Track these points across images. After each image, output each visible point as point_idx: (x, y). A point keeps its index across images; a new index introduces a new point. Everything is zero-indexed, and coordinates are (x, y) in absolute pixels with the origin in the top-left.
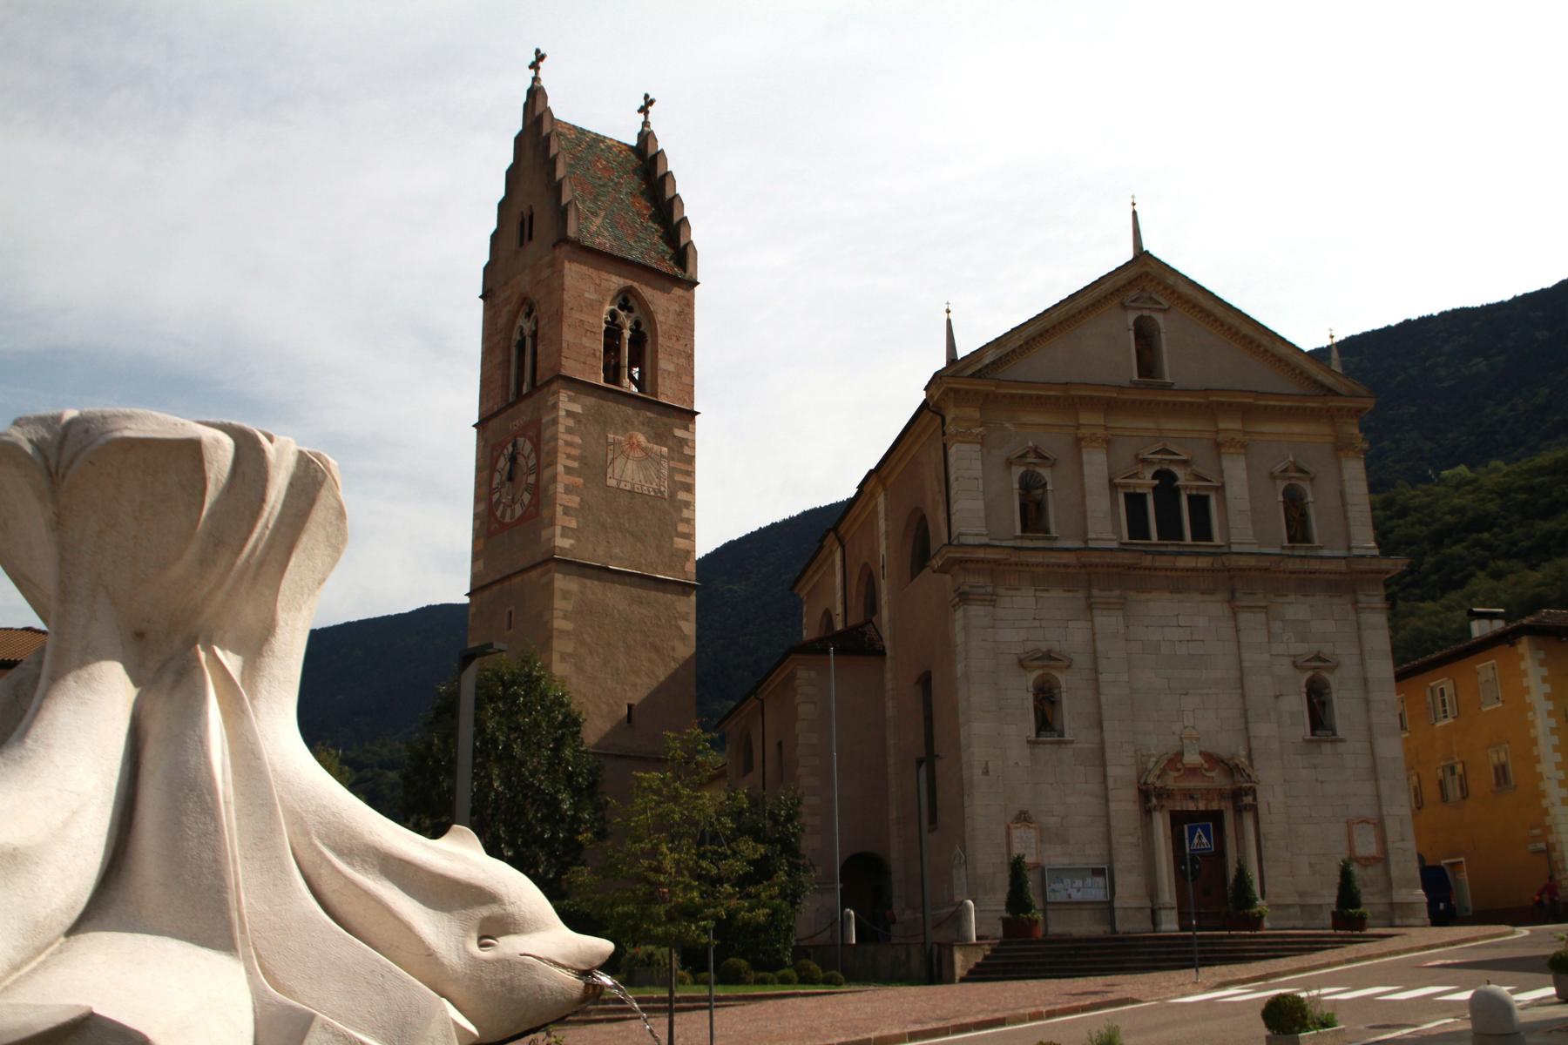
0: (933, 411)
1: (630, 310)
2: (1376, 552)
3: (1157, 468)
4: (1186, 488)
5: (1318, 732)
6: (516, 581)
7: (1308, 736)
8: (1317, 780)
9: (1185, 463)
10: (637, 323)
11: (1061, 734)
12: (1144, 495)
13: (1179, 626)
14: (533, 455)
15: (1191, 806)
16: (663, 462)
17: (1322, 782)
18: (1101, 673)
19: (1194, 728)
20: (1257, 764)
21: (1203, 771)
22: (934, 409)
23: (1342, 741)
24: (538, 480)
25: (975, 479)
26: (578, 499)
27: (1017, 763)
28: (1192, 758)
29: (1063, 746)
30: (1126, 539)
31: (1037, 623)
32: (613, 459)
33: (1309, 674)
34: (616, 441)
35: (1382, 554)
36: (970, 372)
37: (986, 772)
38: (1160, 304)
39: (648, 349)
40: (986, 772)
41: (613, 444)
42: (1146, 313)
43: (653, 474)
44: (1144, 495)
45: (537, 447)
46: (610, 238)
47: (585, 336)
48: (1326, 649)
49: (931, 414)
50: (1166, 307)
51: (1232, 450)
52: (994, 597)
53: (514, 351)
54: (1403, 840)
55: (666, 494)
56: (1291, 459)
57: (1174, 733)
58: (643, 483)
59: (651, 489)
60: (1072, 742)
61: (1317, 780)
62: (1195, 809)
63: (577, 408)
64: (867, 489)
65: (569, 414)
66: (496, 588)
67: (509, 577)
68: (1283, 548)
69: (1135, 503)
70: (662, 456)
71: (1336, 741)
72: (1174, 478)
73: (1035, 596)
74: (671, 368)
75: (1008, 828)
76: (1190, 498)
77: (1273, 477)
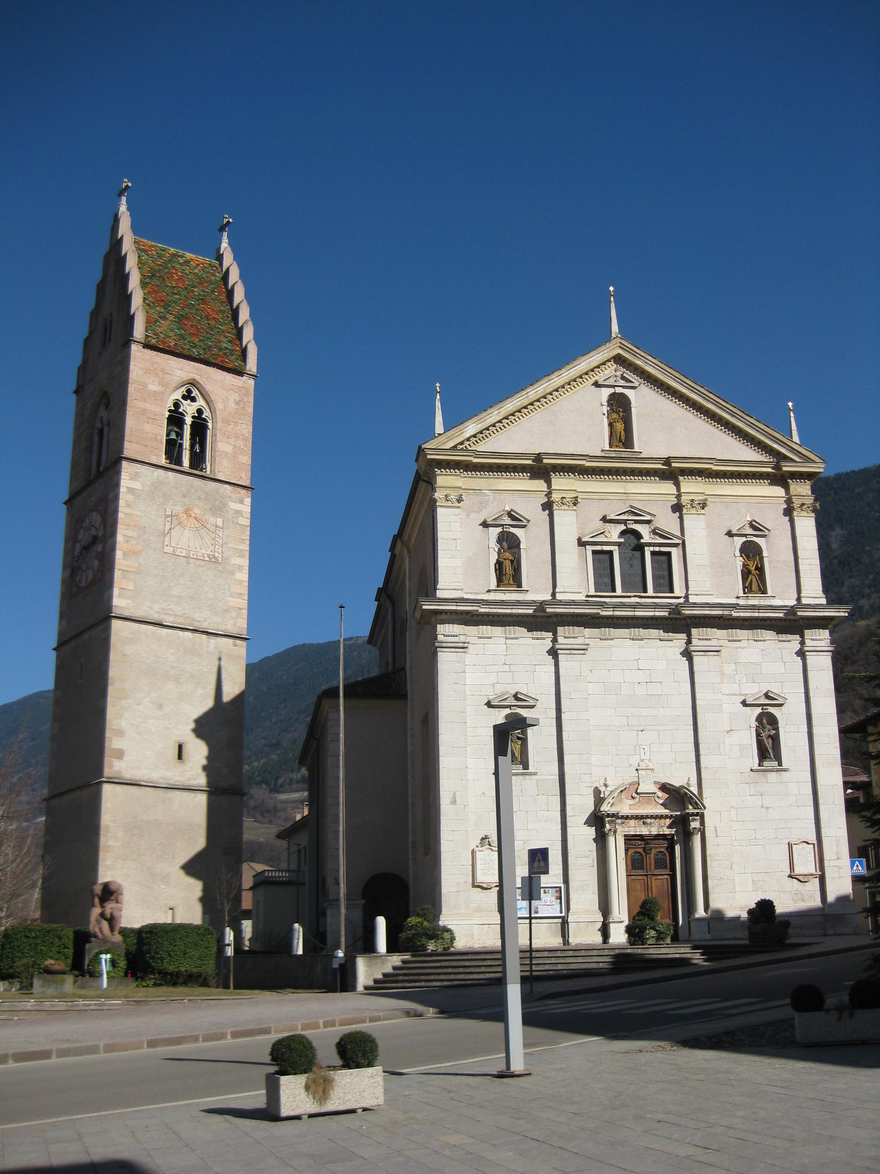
0: (424, 481)
1: (193, 400)
2: (823, 601)
3: (623, 527)
4: (649, 545)
5: (766, 763)
6: (86, 636)
7: (756, 767)
8: (762, 807)
9: (648, 522)
10: (200, 411)
11: (526, 767)
12: (610, 553)
13: (639, 669)
14: (102, 527)
15: (644, 831)
16: (217, 531)
17: (767, 808)
18: (564, 713)
19: (650, 760)
20: (705, 795)
21: (657, 799)
22: (426, 479)
23: (785, 770)
24: (104, 547)
25: (453, 539)
26: (136, 564)
27: (483, 793)
28: (647, 786)
29: (528, 777)
30: (592, 592)
31: (506, 668)
32: (170, 529)
33: (759, 710)
34: (174, 514)
35: (829, 603)
36: (451, 444)
37: (454, 802)
38: (633, 382)
39: (209, 433)
40: (454, 802)
41: (171, 516)
42: (619, 390)
43: (208, 543)
44: (610, 553)
45: (104, 521)
46: (175, 338)
47: (148, 423)
48: (775, 689)
49: (425, 483)
50: (636, 384)
51: (693, 511)
52: (466, 645)
53: (96, 438)
54: (838, 859)
55: (220, 559)
56: (749, 519)
57: (631, 765)
58: (198, 549)
59: (206, 555)
60: (535, 774)
61: (762, 807)
62: (647, 833)
63: (136, 485)
64: (397, 551)
65: (131, 490)
66: (73, 643)
67: (81, 633)
68: (738, 597)
69: (603, 559)
70: (216, 526)
71: (780, 768)
72: (638, 535)
73: (506, 644)
74: (229, 449)
75: (473, 852)
76: (653, 553)
77: (730, 534)
